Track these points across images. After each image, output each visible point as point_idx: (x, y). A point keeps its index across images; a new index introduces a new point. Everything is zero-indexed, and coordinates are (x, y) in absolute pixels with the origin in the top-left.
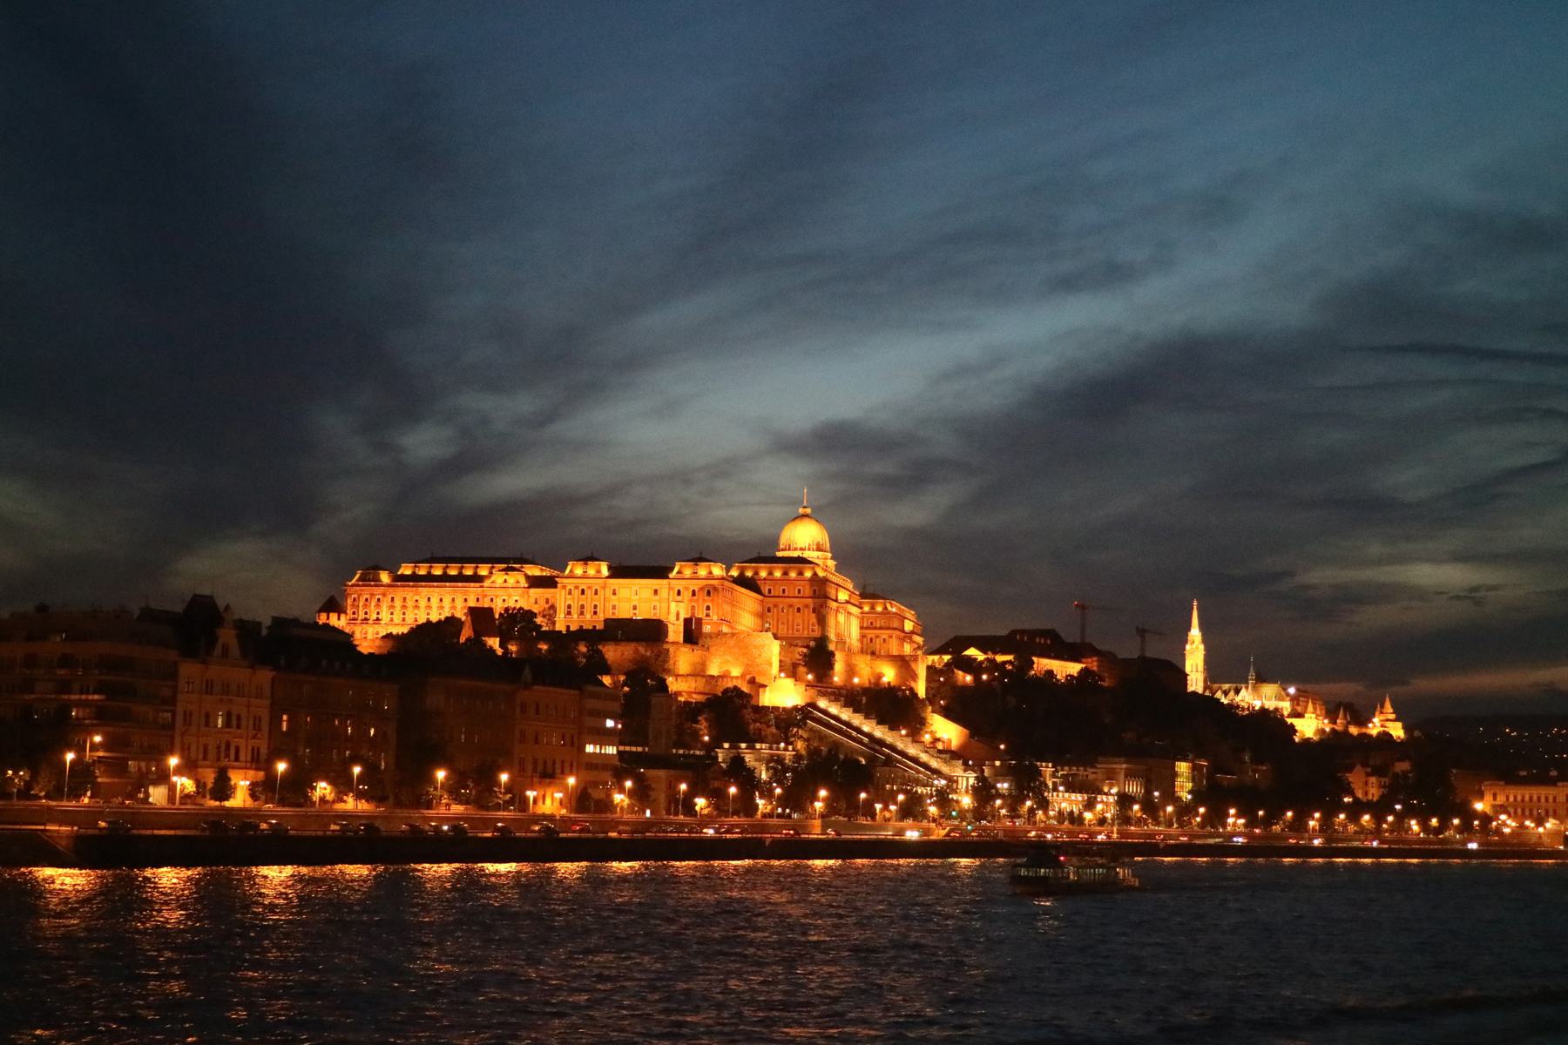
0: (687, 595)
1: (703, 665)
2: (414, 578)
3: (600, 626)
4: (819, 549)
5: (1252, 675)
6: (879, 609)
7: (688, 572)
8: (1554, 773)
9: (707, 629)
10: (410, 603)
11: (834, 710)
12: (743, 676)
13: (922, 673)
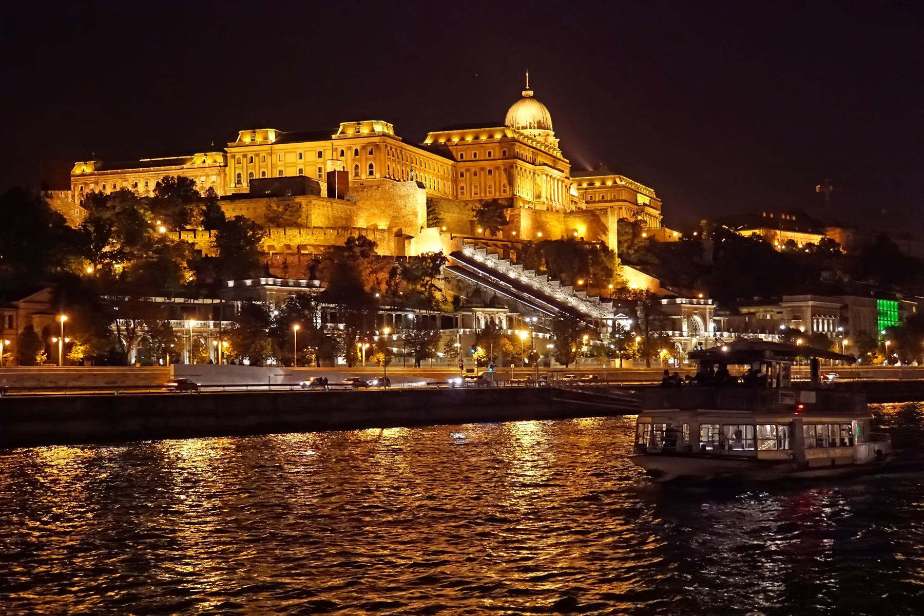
0: (350, 155)
1: (349, 218)
4: (540, 126)
6: (609, 183)
7: (350, 132)
11: (479, 258)
12: (390, 228)
13: (612, 224)
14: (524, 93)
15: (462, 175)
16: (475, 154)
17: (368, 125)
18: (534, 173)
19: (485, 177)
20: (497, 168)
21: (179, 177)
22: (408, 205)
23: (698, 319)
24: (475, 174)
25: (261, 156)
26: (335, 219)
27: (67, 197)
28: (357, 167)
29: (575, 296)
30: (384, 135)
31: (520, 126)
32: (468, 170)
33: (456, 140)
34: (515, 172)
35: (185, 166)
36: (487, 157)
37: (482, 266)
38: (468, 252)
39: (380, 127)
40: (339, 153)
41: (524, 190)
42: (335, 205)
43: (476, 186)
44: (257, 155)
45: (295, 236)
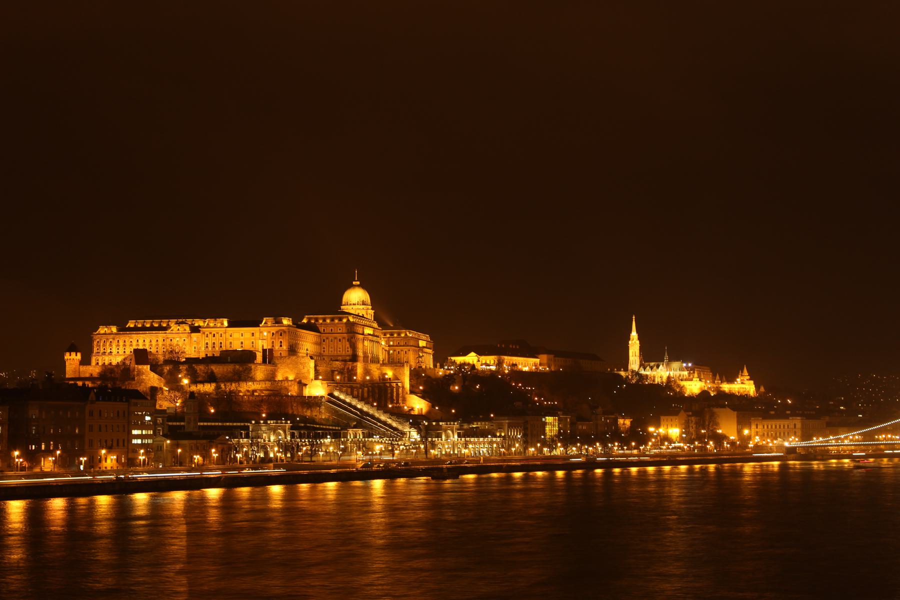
2: (136, 329)
3: (217, 354)
4: (364, 303)
5: (666, 357)
6: (403, 335)
8: (788, 412)
10: (128, 343)
11: (342, 397)
12: (295, 380)
23: (450, 432)
30: (289, 326)
37: (344, 402)
38: (336, 394)
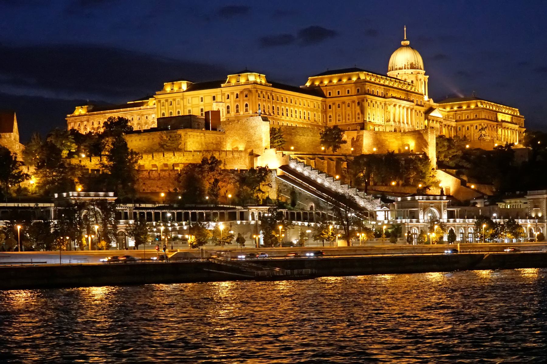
4: (412, 67)
6: (473, 106)
7: (233, 82)
9: (223, 119)
11: (299, 169)
12: (246, 150)
13: (432, 140)
14: (403, 43)
15: (330, 108)
16: (339, 92)
17: (245, 76)
18: (385, 104)
19: (345, 109)
20: (354, 102)
21: (119, 118)
22: (257, 133)
24: (339, 107)
25: (177, 100)
26: (207, 144)
27: (10, 137)
28: (237, 106)
29: (357, 195)
30: (255, 83)
31: (398, 67)
32: (334, 104)
33: (326, 82)
34: (366, 104)
35: (142, 107)
36: (347, 94)
37: (300, 176)
38: (292, 165)
39: (252, 77)
40: (226, 97)
41: (376, 116)
42: (206, 134)
43: (339, 115)
44: (174, 100)
45: (171, 158)
